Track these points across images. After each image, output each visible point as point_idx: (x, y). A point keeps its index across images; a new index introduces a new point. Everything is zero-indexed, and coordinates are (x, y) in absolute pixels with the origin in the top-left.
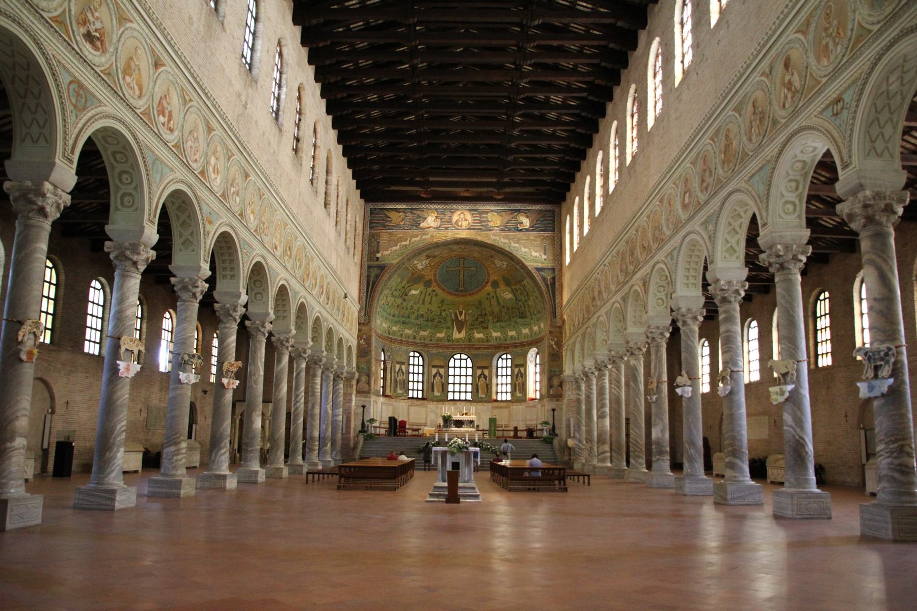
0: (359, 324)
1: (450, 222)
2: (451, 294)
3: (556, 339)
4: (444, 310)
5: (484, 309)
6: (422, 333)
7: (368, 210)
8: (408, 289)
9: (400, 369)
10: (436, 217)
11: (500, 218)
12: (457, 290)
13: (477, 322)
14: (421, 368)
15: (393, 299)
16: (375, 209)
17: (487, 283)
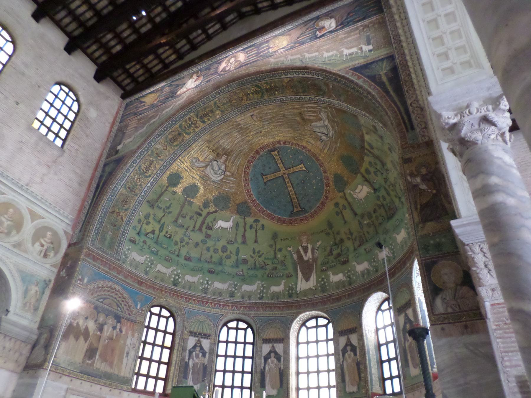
0: (70, 246)
1: (216, 72)
2: (284, 222)
3: (424, 171)
4: (280, 250)
5: (338, 233)
6: (246, 288)
7: (124, 106)
8: (209, 219)
9: (198, 345)
10: (198, 77)
11: (288, 37)
12: (292, 214)
13: (331, 258)
14: (249, 348)
15: (181, 231)
16: (131, 102)
17: (328, 185)
